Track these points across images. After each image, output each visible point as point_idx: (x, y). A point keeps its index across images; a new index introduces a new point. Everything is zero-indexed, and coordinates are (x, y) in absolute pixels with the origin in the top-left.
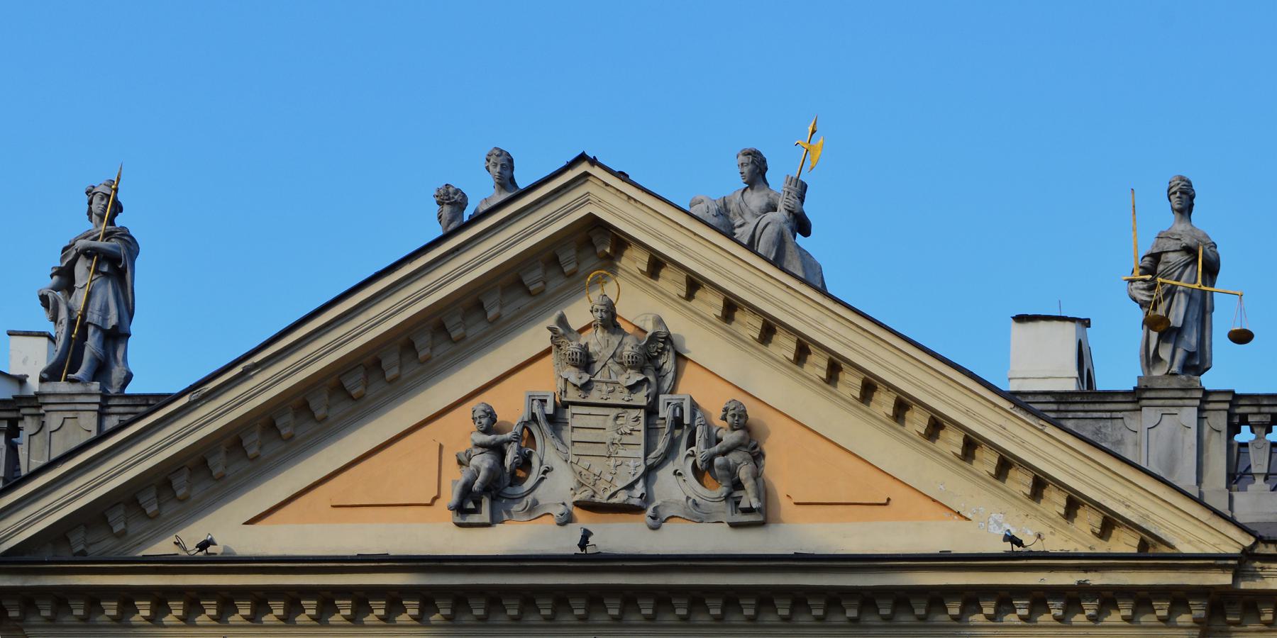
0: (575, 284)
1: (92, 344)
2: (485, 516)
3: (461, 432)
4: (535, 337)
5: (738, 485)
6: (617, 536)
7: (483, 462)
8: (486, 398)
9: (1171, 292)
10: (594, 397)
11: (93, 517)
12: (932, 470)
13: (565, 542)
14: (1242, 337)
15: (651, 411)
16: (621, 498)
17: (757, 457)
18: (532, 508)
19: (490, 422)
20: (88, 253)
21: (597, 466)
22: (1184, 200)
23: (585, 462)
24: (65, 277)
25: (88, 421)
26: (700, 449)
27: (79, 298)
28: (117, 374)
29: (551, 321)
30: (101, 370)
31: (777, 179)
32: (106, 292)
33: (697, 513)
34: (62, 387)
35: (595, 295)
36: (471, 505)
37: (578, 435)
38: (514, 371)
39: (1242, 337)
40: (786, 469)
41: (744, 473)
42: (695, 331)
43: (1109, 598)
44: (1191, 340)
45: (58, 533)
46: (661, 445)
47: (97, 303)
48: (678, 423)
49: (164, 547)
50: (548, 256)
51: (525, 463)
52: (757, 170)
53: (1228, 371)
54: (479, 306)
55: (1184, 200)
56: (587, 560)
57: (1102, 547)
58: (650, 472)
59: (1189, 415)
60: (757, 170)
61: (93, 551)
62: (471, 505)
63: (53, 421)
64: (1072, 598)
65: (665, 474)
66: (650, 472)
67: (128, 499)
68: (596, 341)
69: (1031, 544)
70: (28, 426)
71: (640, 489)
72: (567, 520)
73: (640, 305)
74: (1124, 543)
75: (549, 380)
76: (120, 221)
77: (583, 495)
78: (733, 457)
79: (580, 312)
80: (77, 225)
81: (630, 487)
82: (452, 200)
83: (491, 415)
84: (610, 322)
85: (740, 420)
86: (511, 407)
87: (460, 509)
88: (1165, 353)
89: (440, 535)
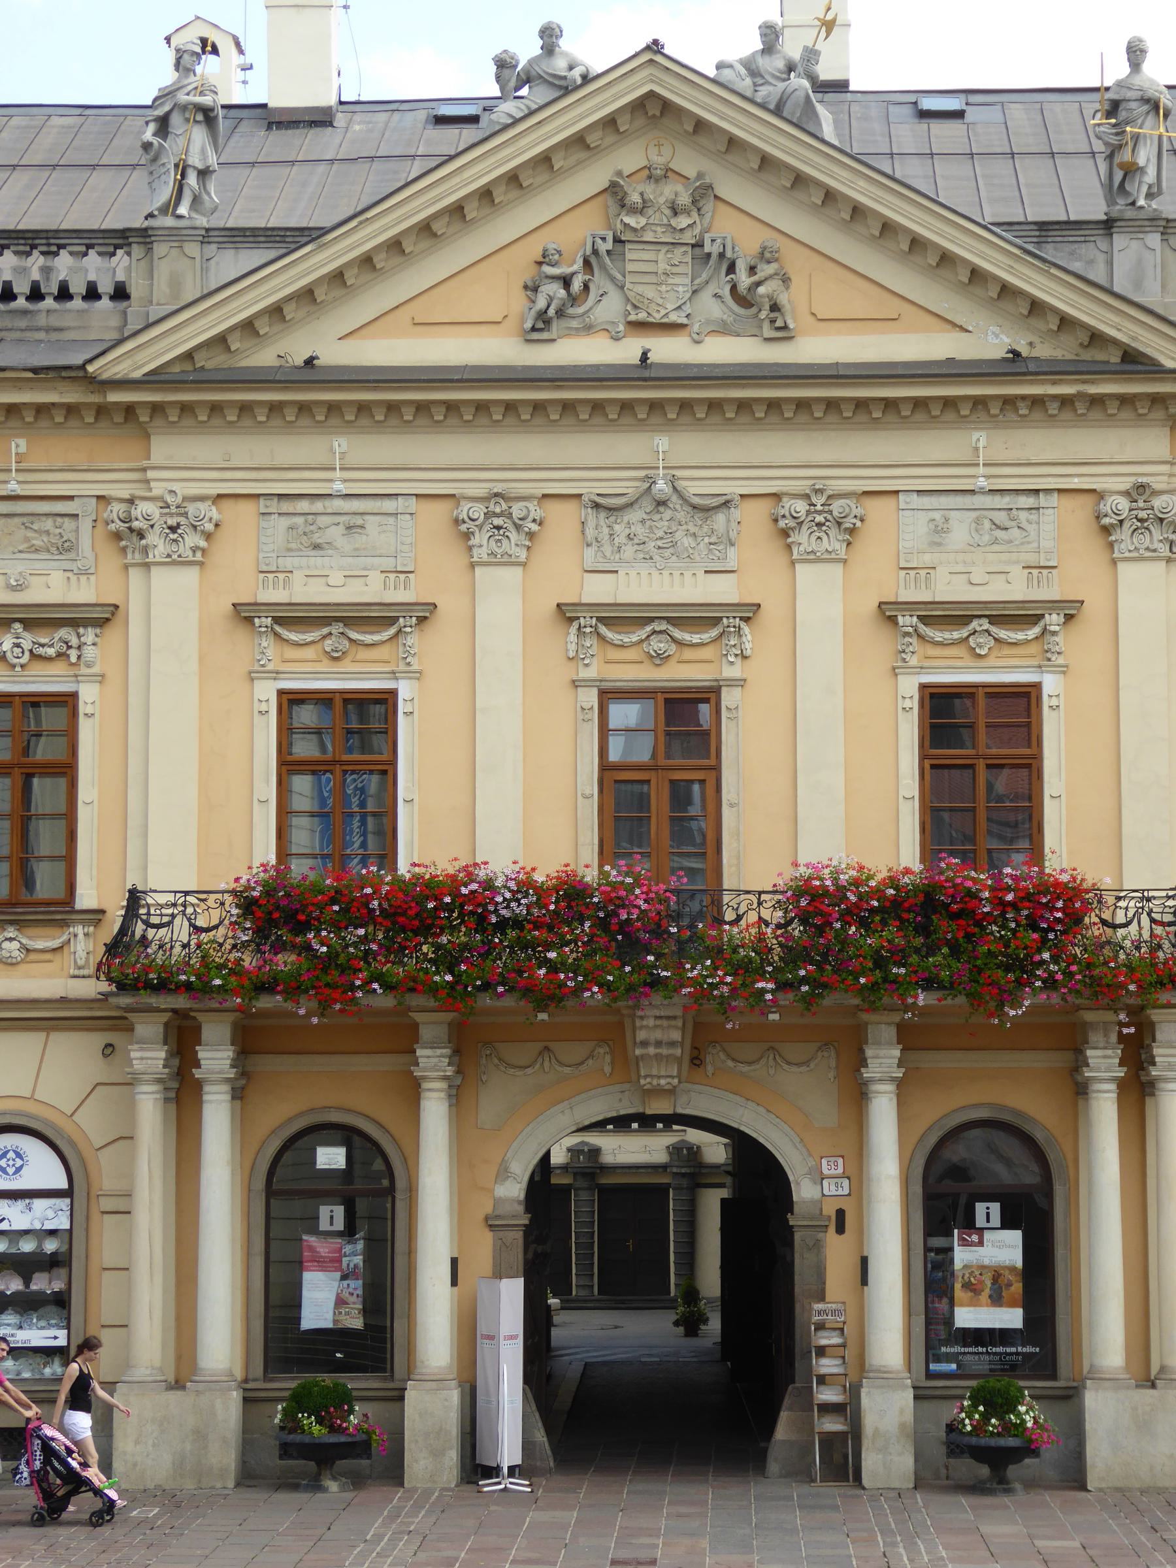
6: (668, 350)
13: (627, 352)
16: (674, 318)
17: (786, 280)
21: (649, 292)
23: (640, 289)
36: (540, 325)
37: (630, 267)
46: (705, 276)
51: (586, 287)
56: (644, 371)
57: (1087, 356)
62: (540, 325)
65: (706, 296)
67: (248, 326)
71: (688, 309)
87: (534, 329)
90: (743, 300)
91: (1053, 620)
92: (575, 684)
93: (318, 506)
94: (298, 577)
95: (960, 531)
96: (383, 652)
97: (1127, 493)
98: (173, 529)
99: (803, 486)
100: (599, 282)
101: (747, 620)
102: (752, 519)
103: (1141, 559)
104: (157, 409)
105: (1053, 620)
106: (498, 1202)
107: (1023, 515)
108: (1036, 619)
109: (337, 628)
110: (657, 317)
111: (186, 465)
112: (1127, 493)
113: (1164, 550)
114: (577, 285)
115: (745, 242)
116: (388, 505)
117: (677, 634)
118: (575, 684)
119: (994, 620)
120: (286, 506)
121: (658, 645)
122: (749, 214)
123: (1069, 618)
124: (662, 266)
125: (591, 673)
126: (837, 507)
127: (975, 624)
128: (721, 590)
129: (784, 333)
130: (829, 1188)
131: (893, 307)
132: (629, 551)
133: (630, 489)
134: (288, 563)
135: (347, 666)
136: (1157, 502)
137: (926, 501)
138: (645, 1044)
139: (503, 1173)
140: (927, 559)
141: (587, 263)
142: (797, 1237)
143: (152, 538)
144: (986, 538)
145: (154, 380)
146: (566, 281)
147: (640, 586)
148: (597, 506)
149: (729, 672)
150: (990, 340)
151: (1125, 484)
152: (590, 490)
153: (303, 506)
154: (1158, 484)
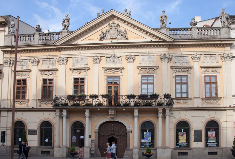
0: (110, 20)
1: (66, 27)
2: (102, 40)
3: (100, 33)
4: (107, 24)
5: (126, 36)
6: (114, 41)
7: (103, 35)
8: (102, 30)
9: (164, 20)
10: (112, 29)
11: (68, 41)
12: (143, 35)
13: (110, 41)
14: (170, 23)
15: (117, 30)
16: (115, 38)
18: (106, 39)
19: (103, 32)
20: (66, 20)
21: (112, 35)
22: (164, 12)
23: (111, 35)
24: (64, 22)
25: (66, 33)
26: (122, 34)
27: (65, 23)
28: (68, 29)
29: (109, 23)
30: (67, 29)
31: (128, 11)
32: (67, 22)
33: (121, 39)
34: (64, 31)
35: (113, 21)
36: (101, 39)
38: (105, 28)
39: (170, 23)
40: (129, 35)
41: (126, 35)
42: (121, 24)
43: (160, 45)
44: (165, 24)
45: (64, 43)
46: (118, 33)
47: (67, 24)
48: (120, 31)
49: (73, 43)
50: (108, 18)
51: (106, 35)
52: (126, 11)
53: (168, 26)
54: (102, 22)
55: (164, 12)
58: (117, 35)
59: (166, 30)
60: (126, 11)
61: (67, 44)
62: (101, 39)
63: (63, 33)
64: (157, 45)
65: (118, 36)
66: (117, 35)
67: (71, 40)
68: (112, 25)
69: (153, 41)
70: (61, 34)
71: (116, 37)
72: (110, 40)
73: (116, 22)
74: (162, 40)
75: (108, 28)
76: (68, 17)
77: (111, 38)
78: (125, 34)
79: (111, 22)
80: (65, 17)
81: (115, 37)
82: (98, 14)
83: (103, 31)
84: (114, 23)
85: (125, 31)
86: (105, 31)
87: (100, 39)
88: (163, 25)
89: (98, 41)
90: (122, 35)
91: (155, 68)
92: (104, 76)
93: (78, 58)
94: (75, 66)
95: (146, 59)
96: (84, 73)
97: (163, 55)
98: (63, 61)
99: (129, 55)
100: (107, 34)
101: (123, 69)
102: (124, 58)
103: (165, 62)
104: (62, 48)
105: (155, 68)
106: (95, 130)
107: (152, 58)
108: (153, 68)
109: (79, 70)
110: (113, 38)
111: (65, 54)
112: (163, 55)
113: (167, 61)
114: (105, 35)
115: (123, 30)
116: (85, 58)
117: (115, 70)
118: (104, 76)
119: (149, 68)
120: (75, 58)
121: (113, 71)
122: (123, 27)
123: (157, 68)
124: (114, 33)
125: (106, 75)
126: (132, 57)
127: (147, 69)
128: (120, 66)
129: (127, 39)
130: (130, 128)
131: (139, 36)
132: (110, 62)
133: (110, 56)
134: (74, 64)
135: (80, 74)
136: (166, 56)
137: (142, 56)
138: (110, 112)
139: (96, 127)
140: (142, 62)
141: (106, 33)
142: (127, 133)
143: (61, 62)
144: (148, 60)
145: (61, 45)
146: (103, 34)
147: (111, 65)
148: (107, 57)
149: (120, 74)
150: (148, 39)
151: (163, 54)
152: (106, 56)
153: (76, 58)
154: (166, 54)
